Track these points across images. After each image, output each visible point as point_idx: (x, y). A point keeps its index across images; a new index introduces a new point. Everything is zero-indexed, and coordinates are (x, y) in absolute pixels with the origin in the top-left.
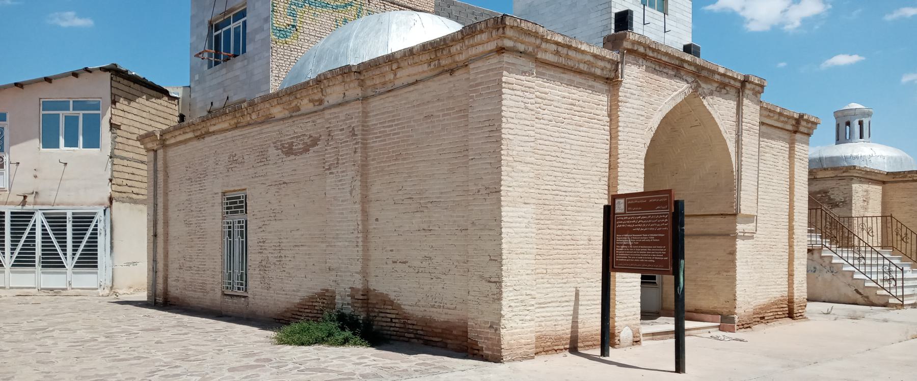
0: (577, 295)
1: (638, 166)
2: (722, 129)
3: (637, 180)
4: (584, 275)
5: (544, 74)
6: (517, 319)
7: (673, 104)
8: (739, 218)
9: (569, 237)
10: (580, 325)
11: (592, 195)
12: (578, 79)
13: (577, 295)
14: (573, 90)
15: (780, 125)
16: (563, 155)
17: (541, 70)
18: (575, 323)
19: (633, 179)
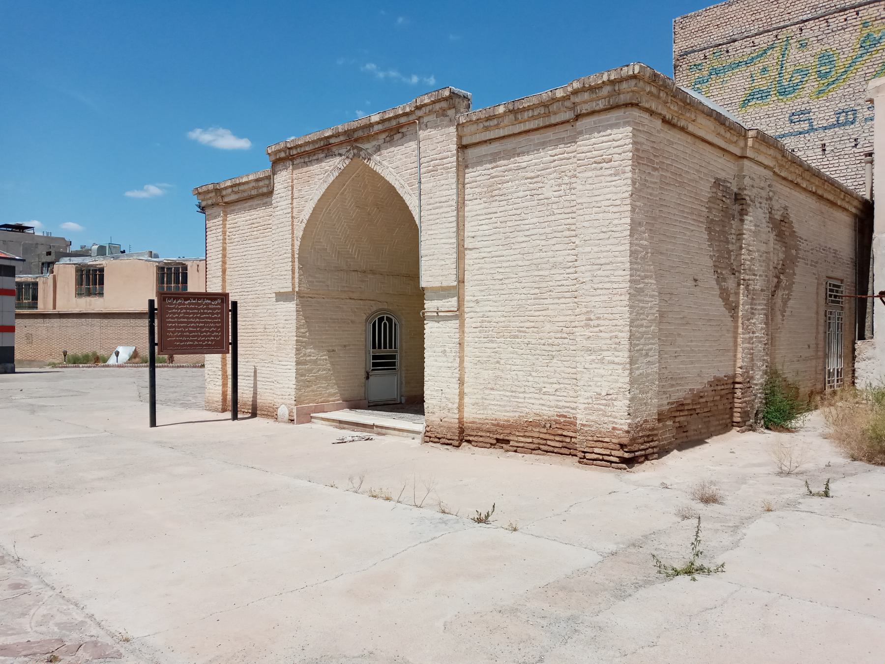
0: (255, 372)
1: (286, 260)
2: (397, 186)
3: (285, 273)
4: (260, 357)
5: (234, 210)
6: (212, 383)
7: (326, 186)
8: (427, 294)
9: (250, 327)
10: (258, 397)
11: (266, 292)
12: (256, 202)
13: (255, 372)
14: (253, 212)
15: (540, 123)
16: (247, 264)
17: (232, 208)
18: (255, 393)
19: (282, 273)
